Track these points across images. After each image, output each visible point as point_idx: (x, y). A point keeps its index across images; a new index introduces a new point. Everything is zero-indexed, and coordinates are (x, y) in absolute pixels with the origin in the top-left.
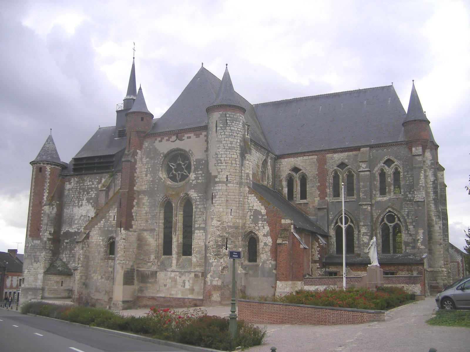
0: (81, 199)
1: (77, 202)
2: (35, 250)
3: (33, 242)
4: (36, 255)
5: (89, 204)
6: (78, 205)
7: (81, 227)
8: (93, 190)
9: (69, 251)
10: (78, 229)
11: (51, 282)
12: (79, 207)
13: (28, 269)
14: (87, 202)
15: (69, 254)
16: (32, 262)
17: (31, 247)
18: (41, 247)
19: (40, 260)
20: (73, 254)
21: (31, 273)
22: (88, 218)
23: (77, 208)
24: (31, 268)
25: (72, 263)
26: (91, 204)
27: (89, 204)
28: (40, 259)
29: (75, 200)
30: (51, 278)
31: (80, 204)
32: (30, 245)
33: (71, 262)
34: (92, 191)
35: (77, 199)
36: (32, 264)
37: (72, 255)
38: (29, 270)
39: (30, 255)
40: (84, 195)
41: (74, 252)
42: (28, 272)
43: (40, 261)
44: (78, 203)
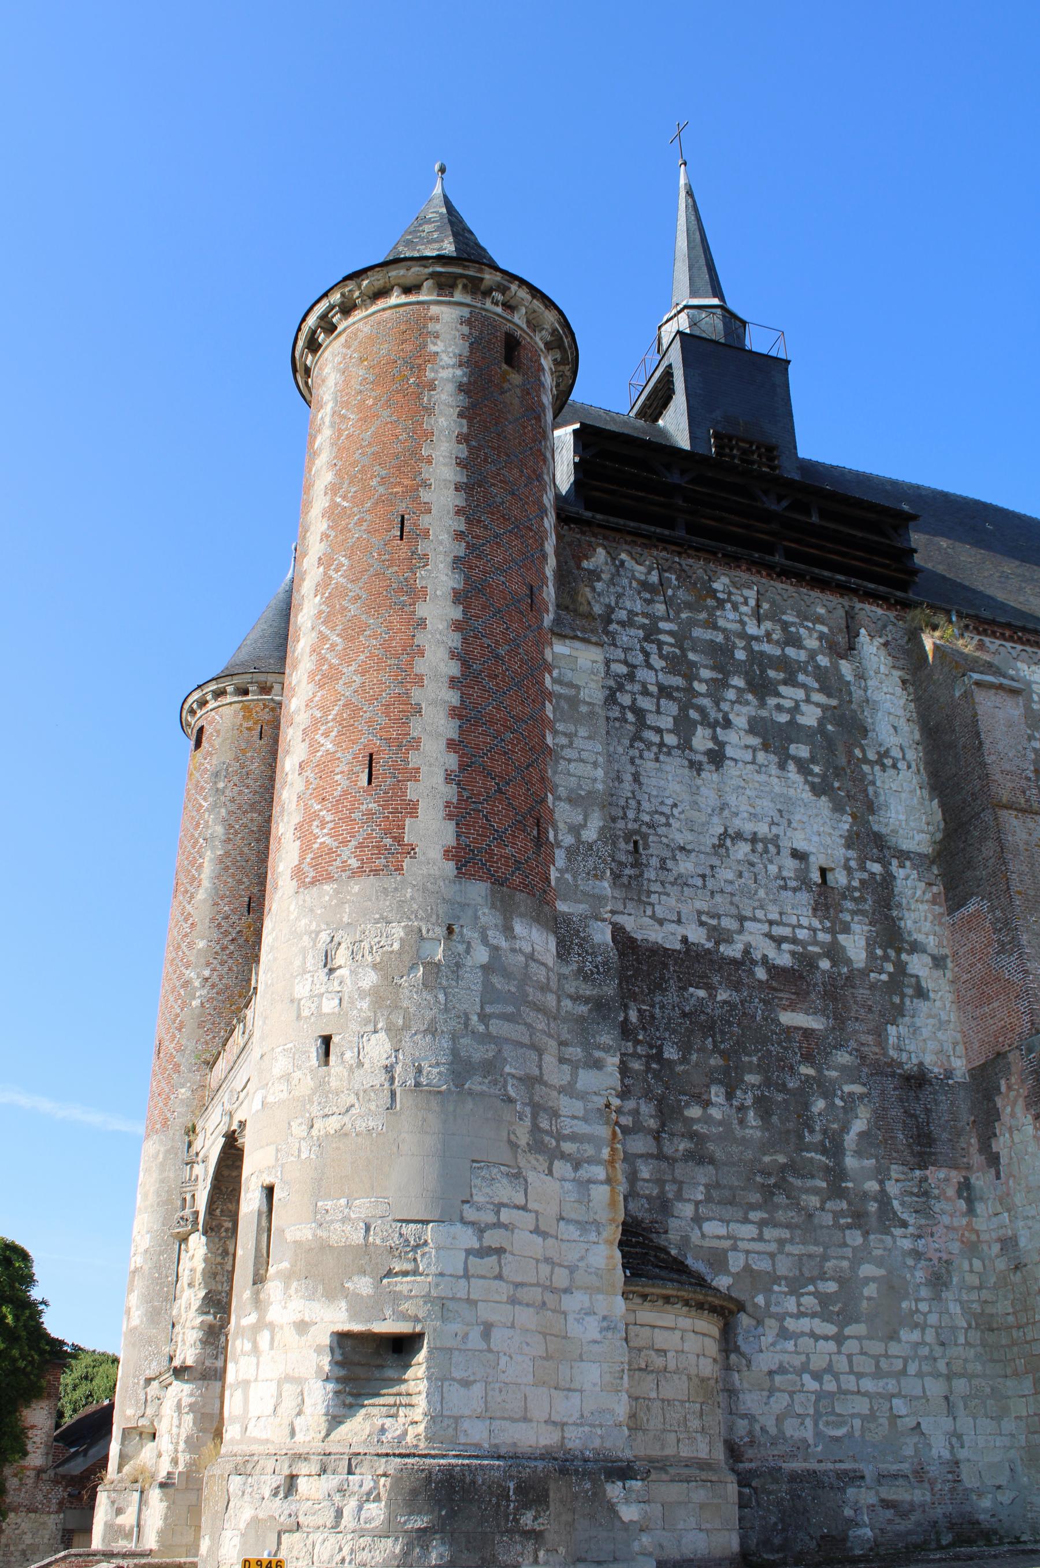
0: (701, 710)
1: (666, 722)
2: (530, 1016)
3: (508, 930)
4: (540, 1080)
5: (782, 766)
6: (686, 745)
7: (742, 919)
8: (801, 678)
9: (647, 1109)
10: (720, 935)
11: (668, 1391)
12: (696, 767)
13: (480, 1230)
14: (766, 747)
15: (657, 1137)
16: (513, 1146)
17: (497, 981)
18: (567, 1004)
19: (573, 1138)
20: (692, 1135)
21: (511, 1268)
22: (790, 865)
23: (674, 766)
24: (505, 1216)
25: (698, 1220)
26: (803, 767)
27: (782, 766)
28: (568, 1126)
29: (646, 703)
30: (661, 1339)
31: (702, 740)
32: (481, 955)
33: (687, 1210)
34: (791, 681)
35: (671, 708)
36: (517, 1176)
37: (683, 1145)
38: (492, 1238)
39: (490, 1068)
40: (731, 694)
41: (707, 1120)
42: (483, 1252)
43: (568, 1147)
44: (684, 727)
